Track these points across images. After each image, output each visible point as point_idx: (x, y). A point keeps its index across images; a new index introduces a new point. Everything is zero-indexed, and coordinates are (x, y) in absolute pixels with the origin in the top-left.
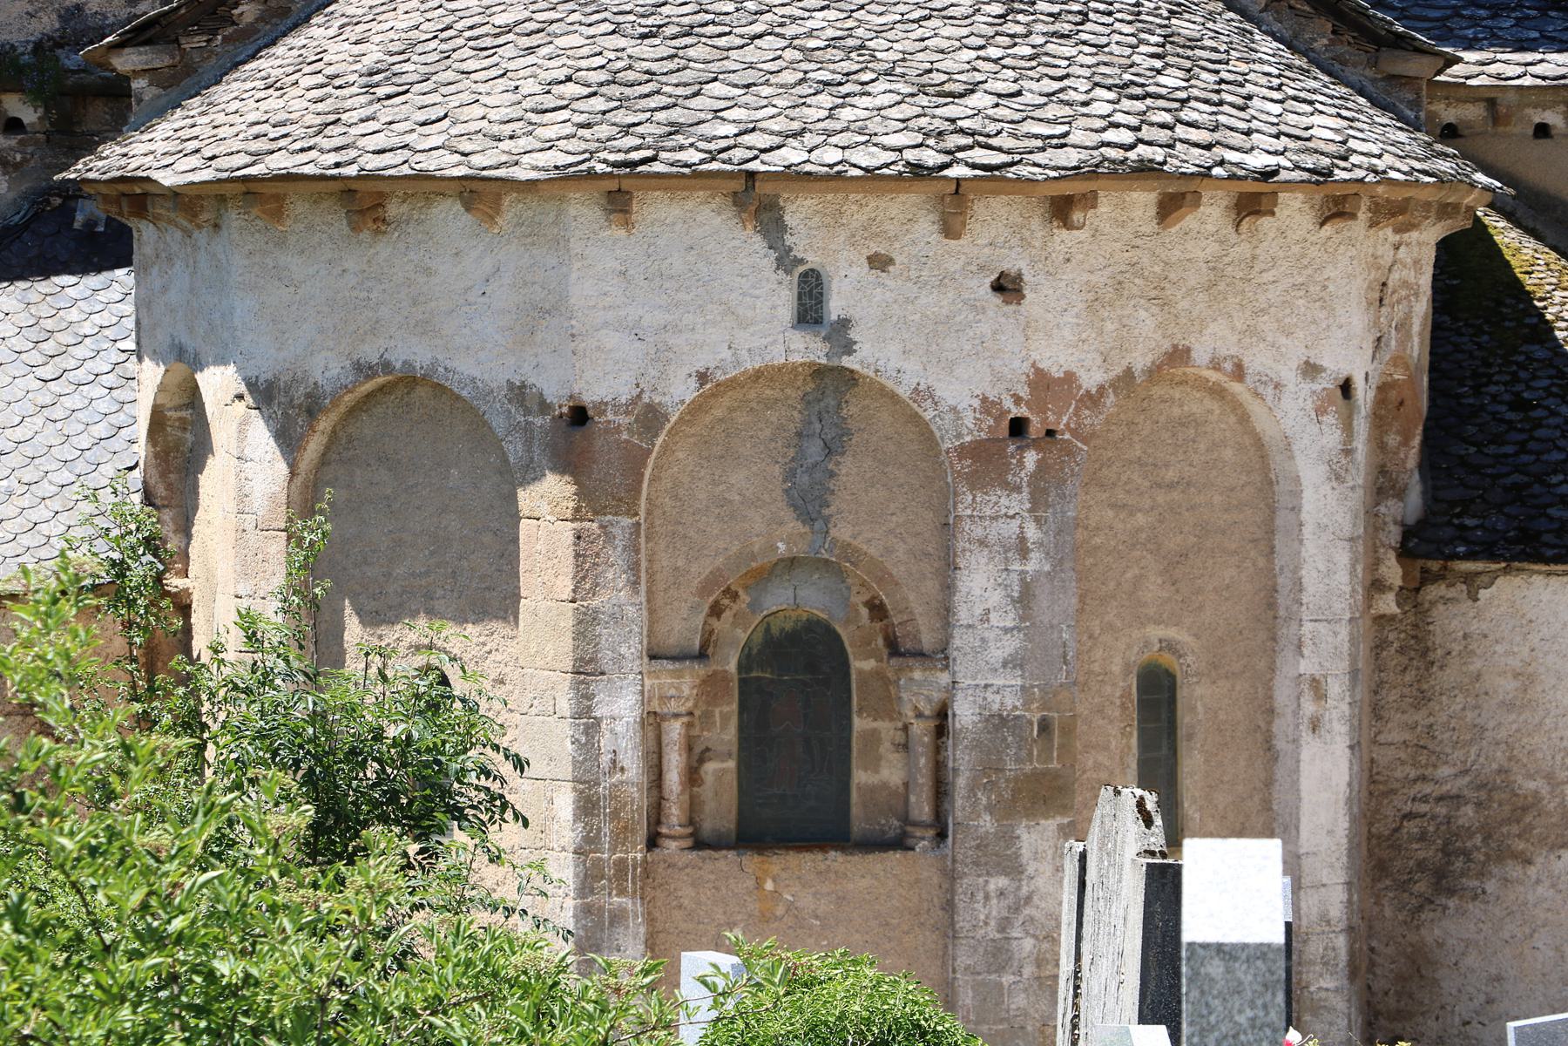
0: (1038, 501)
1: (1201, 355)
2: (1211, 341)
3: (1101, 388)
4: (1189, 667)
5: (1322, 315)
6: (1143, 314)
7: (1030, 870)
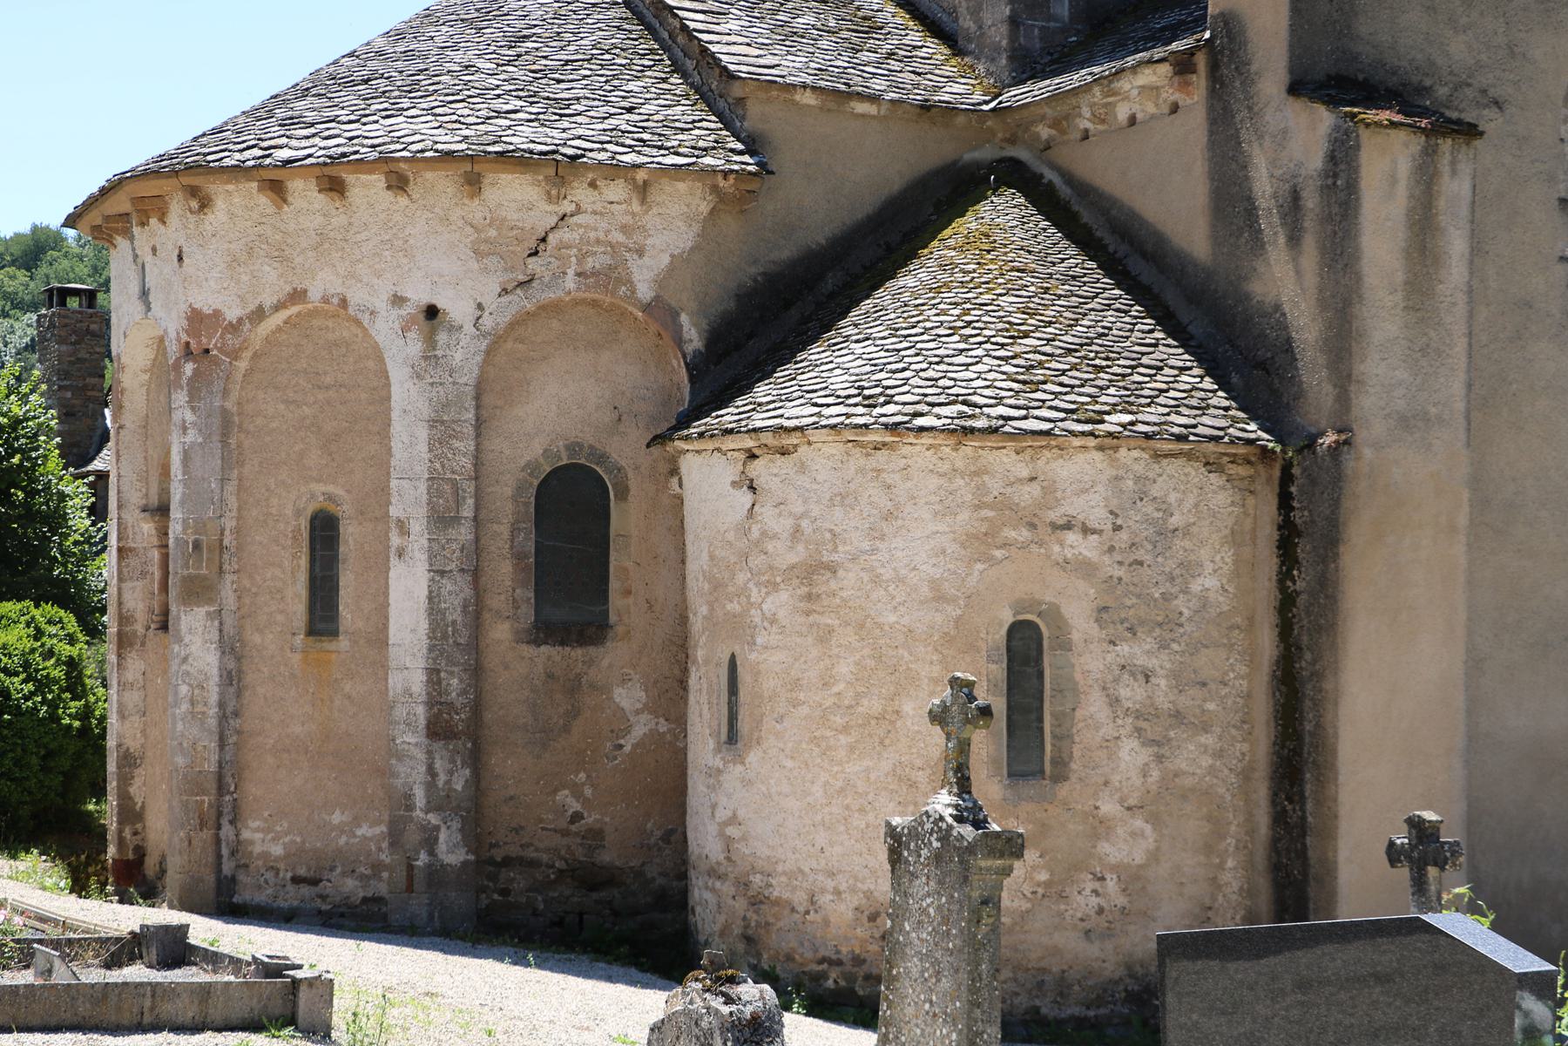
1: (315, 294)
3: (240, 320)
4: (345, 511)
5: (405, 261)
6: (267, 268)
7: (186, 640)
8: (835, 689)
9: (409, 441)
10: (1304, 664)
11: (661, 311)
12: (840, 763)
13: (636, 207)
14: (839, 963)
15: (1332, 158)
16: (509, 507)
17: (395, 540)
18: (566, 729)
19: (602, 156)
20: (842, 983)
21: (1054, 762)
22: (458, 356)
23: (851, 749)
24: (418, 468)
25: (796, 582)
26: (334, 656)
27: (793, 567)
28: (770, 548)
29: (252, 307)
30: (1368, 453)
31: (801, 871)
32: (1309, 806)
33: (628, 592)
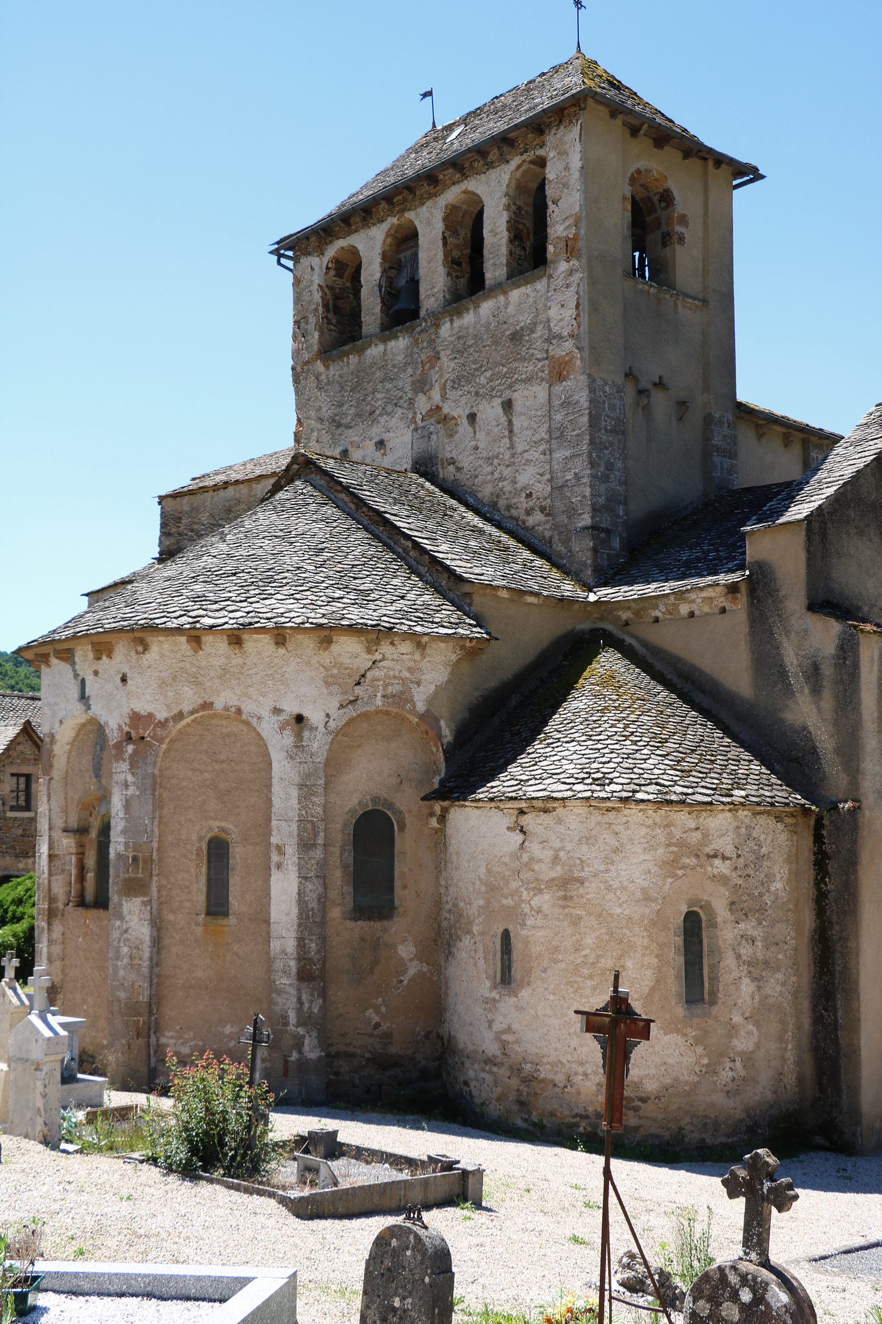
0: (133, 765)
1: (219, 705)
2: (223, 699)
3: (167, 720)
4: (234, 837)
5: (282, 687)
6: (186, 689)
7: (127, 918)
8: (583, 953)
9: (285, 798)
10: (834, 932)
11: (429, 718)
12: (587, 997)
13: (417, 657)
14: (587, 1117)
15: (841, 648)
16: (340, 836)
17: (275, 858)
18: (371, 971)
19: (405, 628)
20: (589, 1129)
21: (710, 994)
22: (316, 746)
23: (594, 988)
24: (291, 814)
25: (555, 888)
26: (226, 929)
27: (553, 880)
28: (536, 867)
29: (175, 712)
30: (867, 813)
31: (560, 1061)
32: (840, 1013)
33: (405, 887)
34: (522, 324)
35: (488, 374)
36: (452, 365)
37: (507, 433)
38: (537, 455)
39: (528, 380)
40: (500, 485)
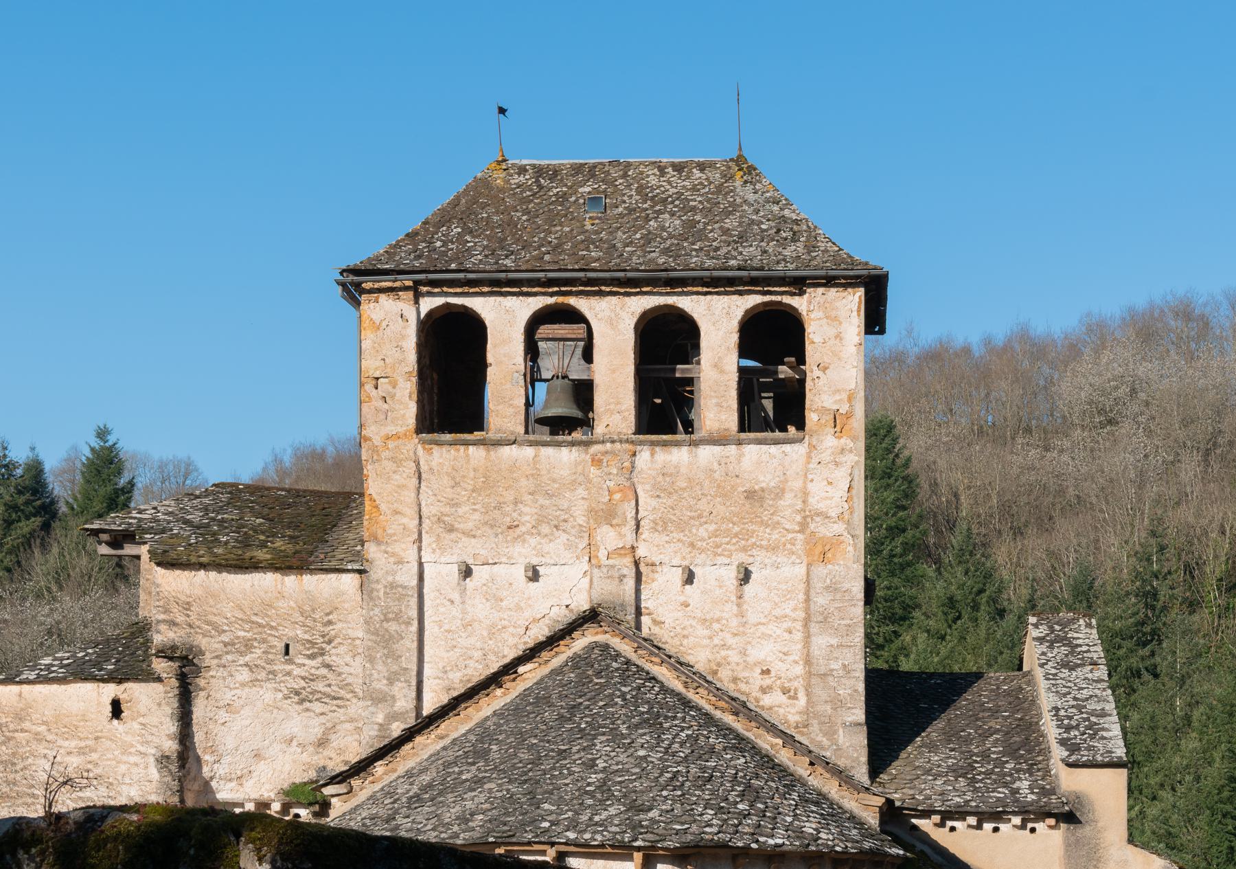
34: (764, 485)
35: (712, 527)
36: (654, 503)
37: (734, 598)
38: (779, 632)
39: (773, 548)
40: (723, 653)
